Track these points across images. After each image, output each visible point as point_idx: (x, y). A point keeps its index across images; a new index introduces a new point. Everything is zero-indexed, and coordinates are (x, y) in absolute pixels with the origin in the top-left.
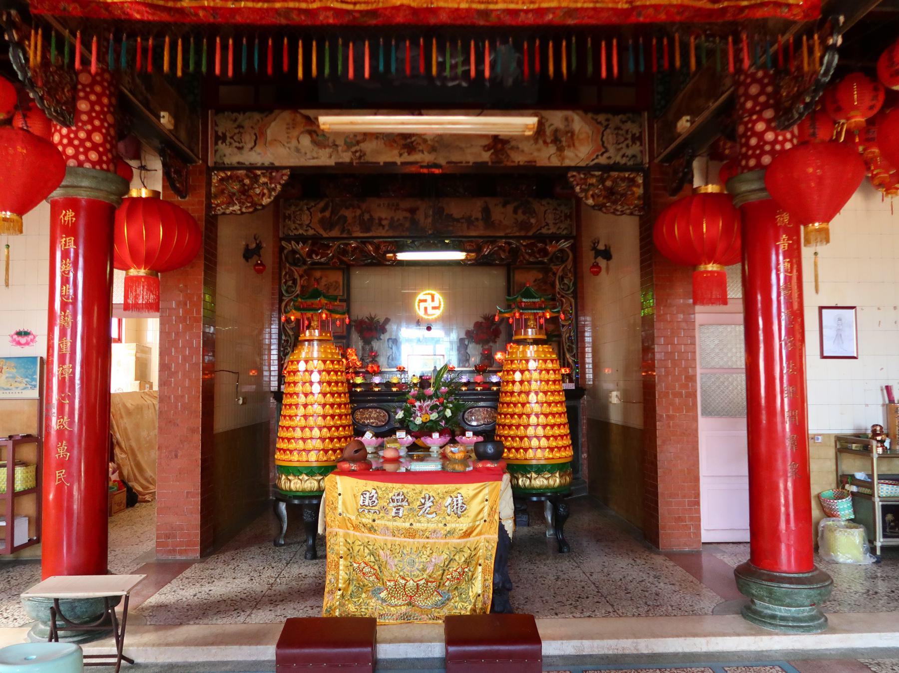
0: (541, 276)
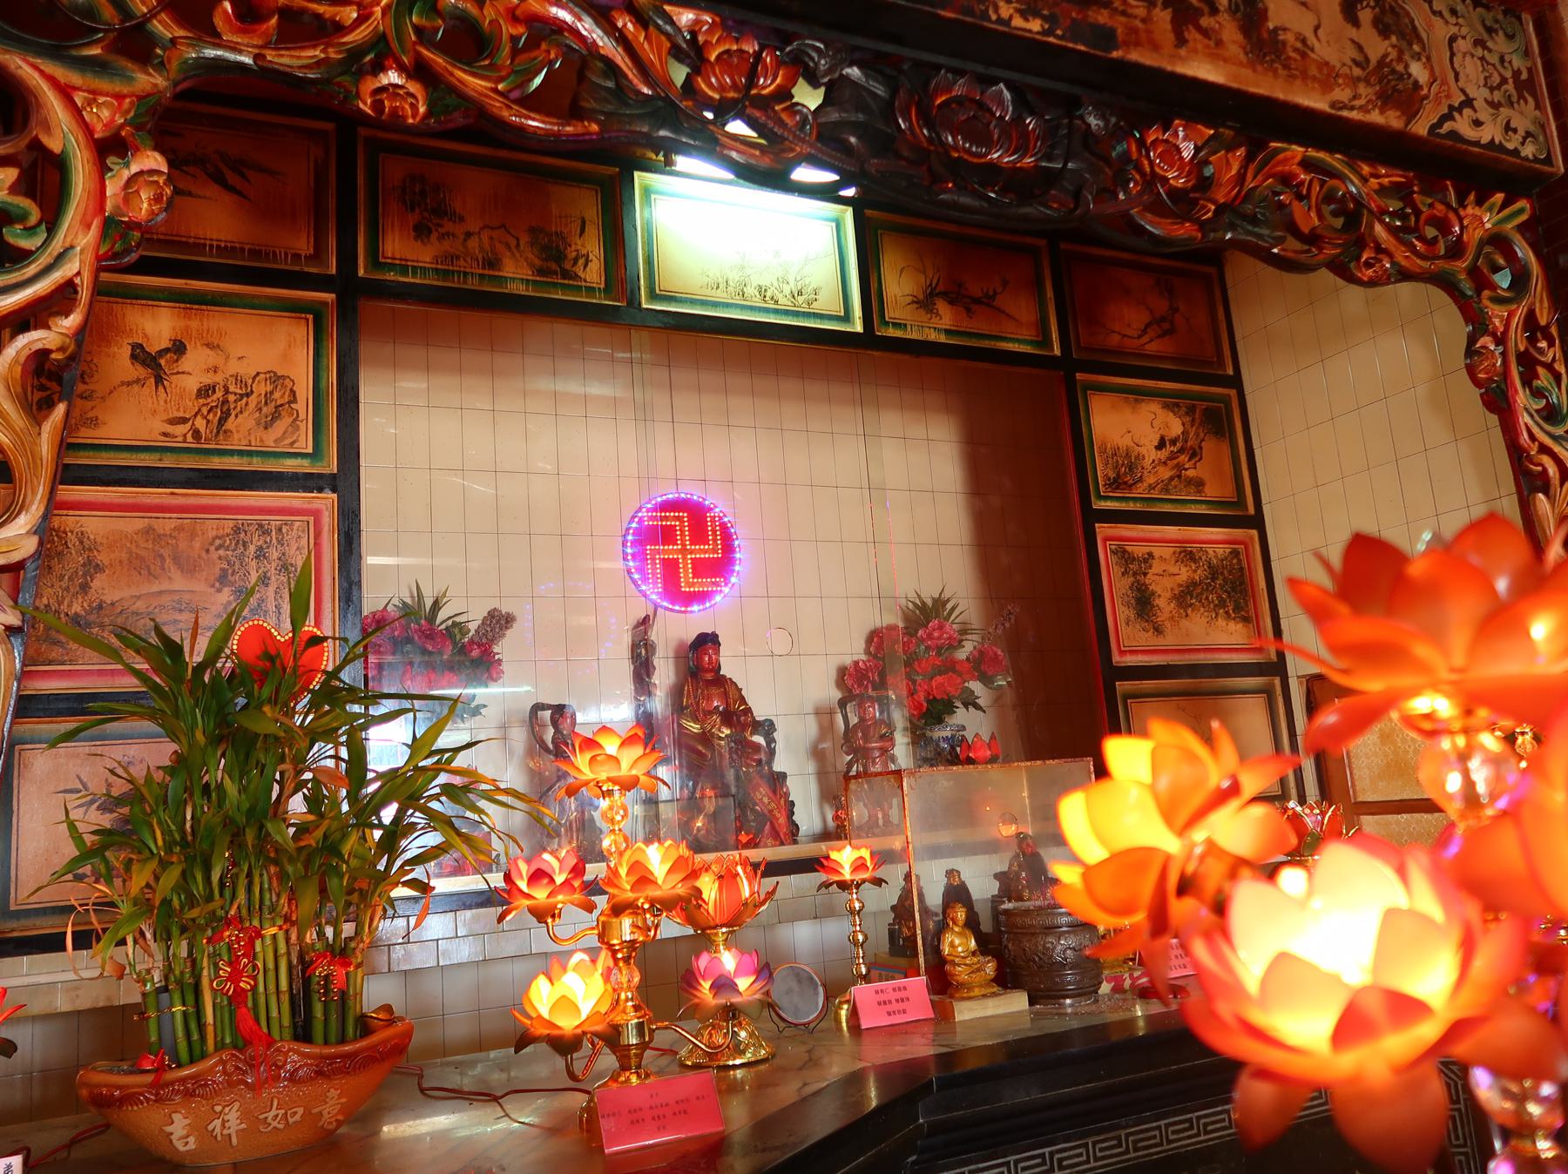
0: (1176, 427)
